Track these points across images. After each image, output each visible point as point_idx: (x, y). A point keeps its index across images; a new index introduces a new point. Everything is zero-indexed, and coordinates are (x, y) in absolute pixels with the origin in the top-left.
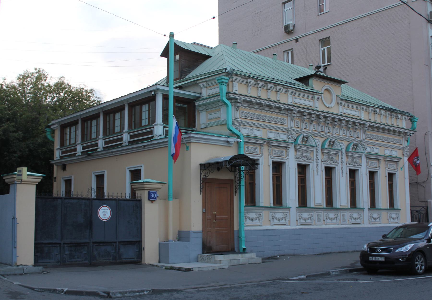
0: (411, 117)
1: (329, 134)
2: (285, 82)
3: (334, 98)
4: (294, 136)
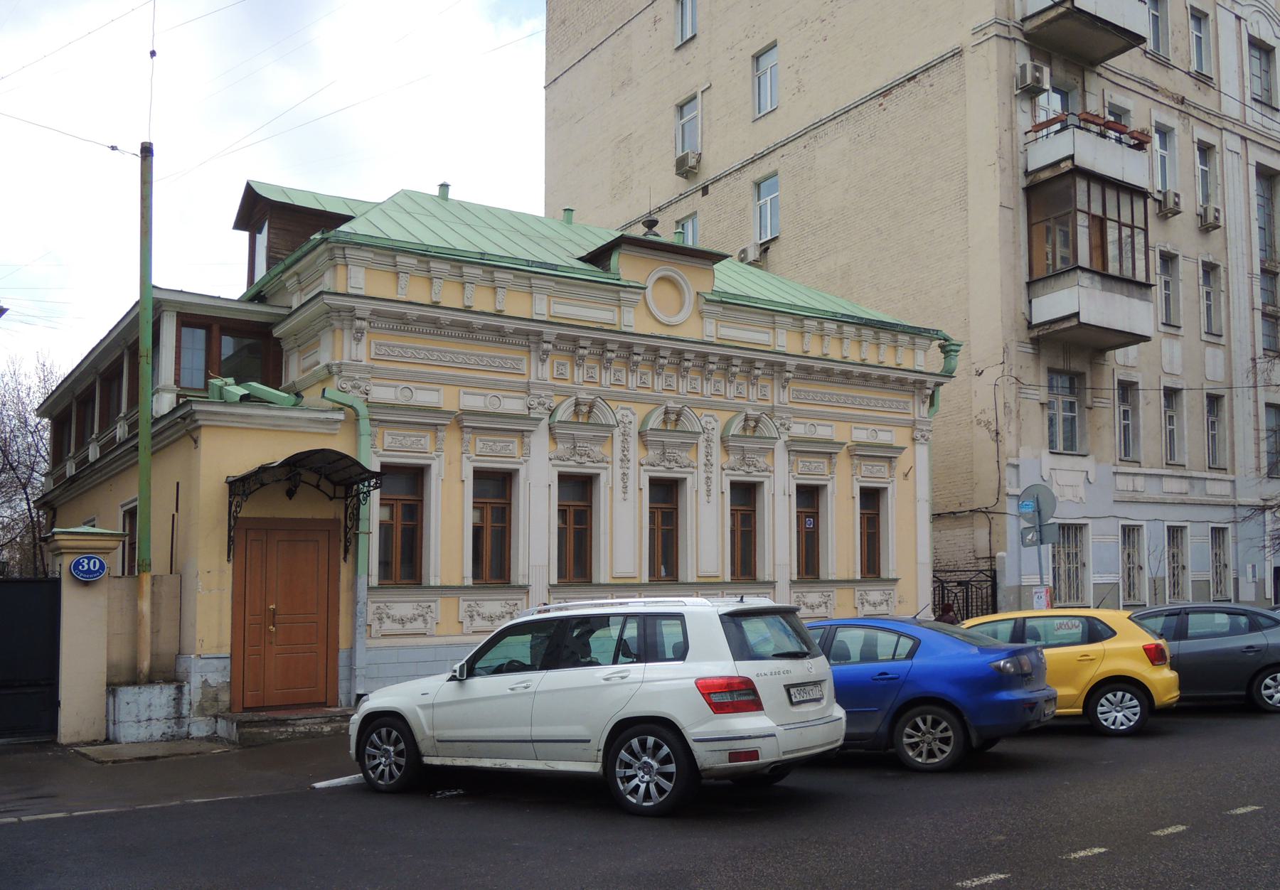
0: (942, 341)
1: (665, 394)
3: (690, 298)
4: (787, 422)
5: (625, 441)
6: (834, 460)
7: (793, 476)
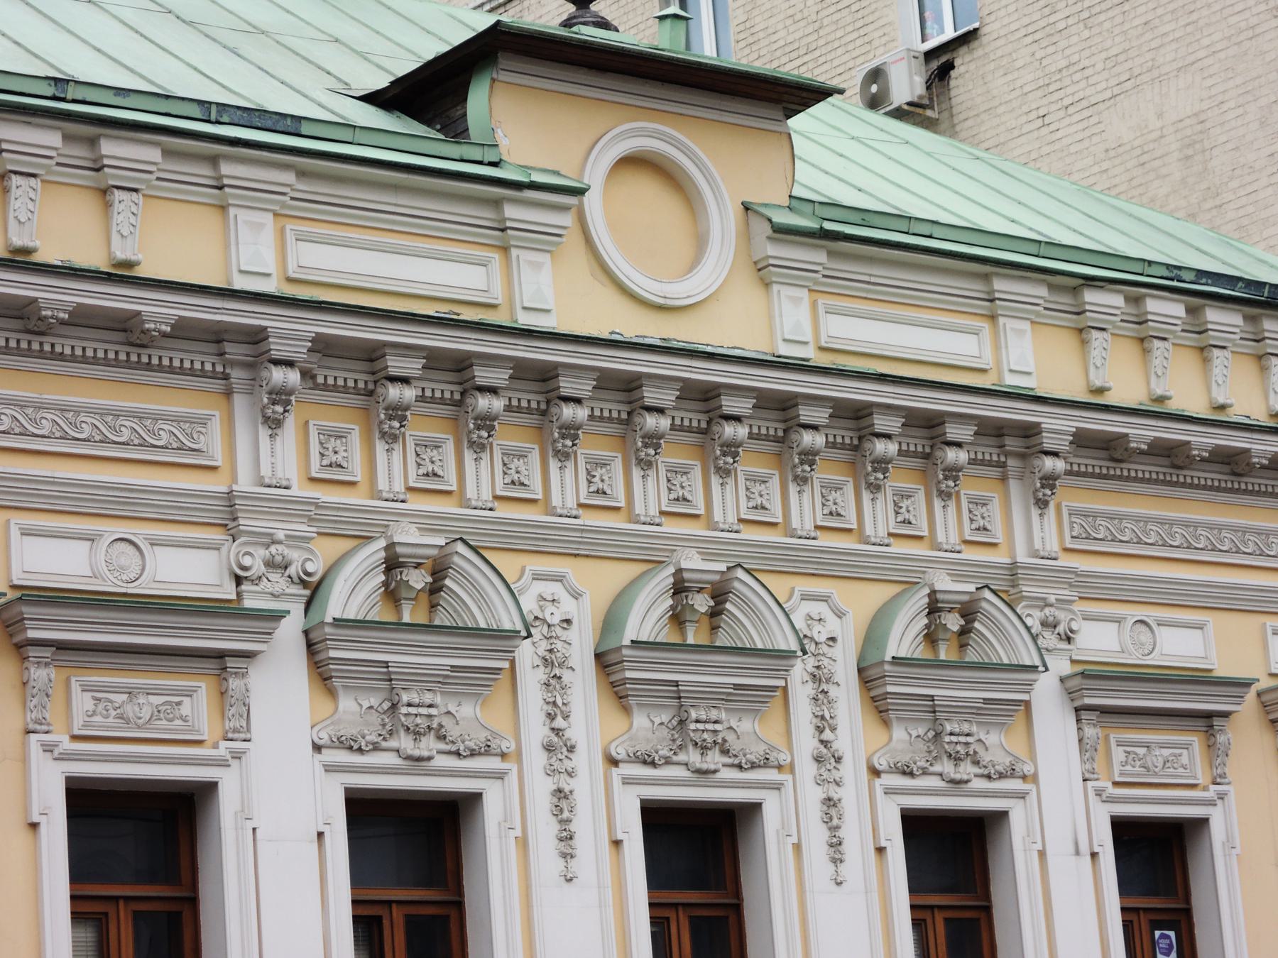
1: (672, 527)
2: (196, 111)
5: (553, 683)
6: (1221, 738)
7: (1099, 793)
